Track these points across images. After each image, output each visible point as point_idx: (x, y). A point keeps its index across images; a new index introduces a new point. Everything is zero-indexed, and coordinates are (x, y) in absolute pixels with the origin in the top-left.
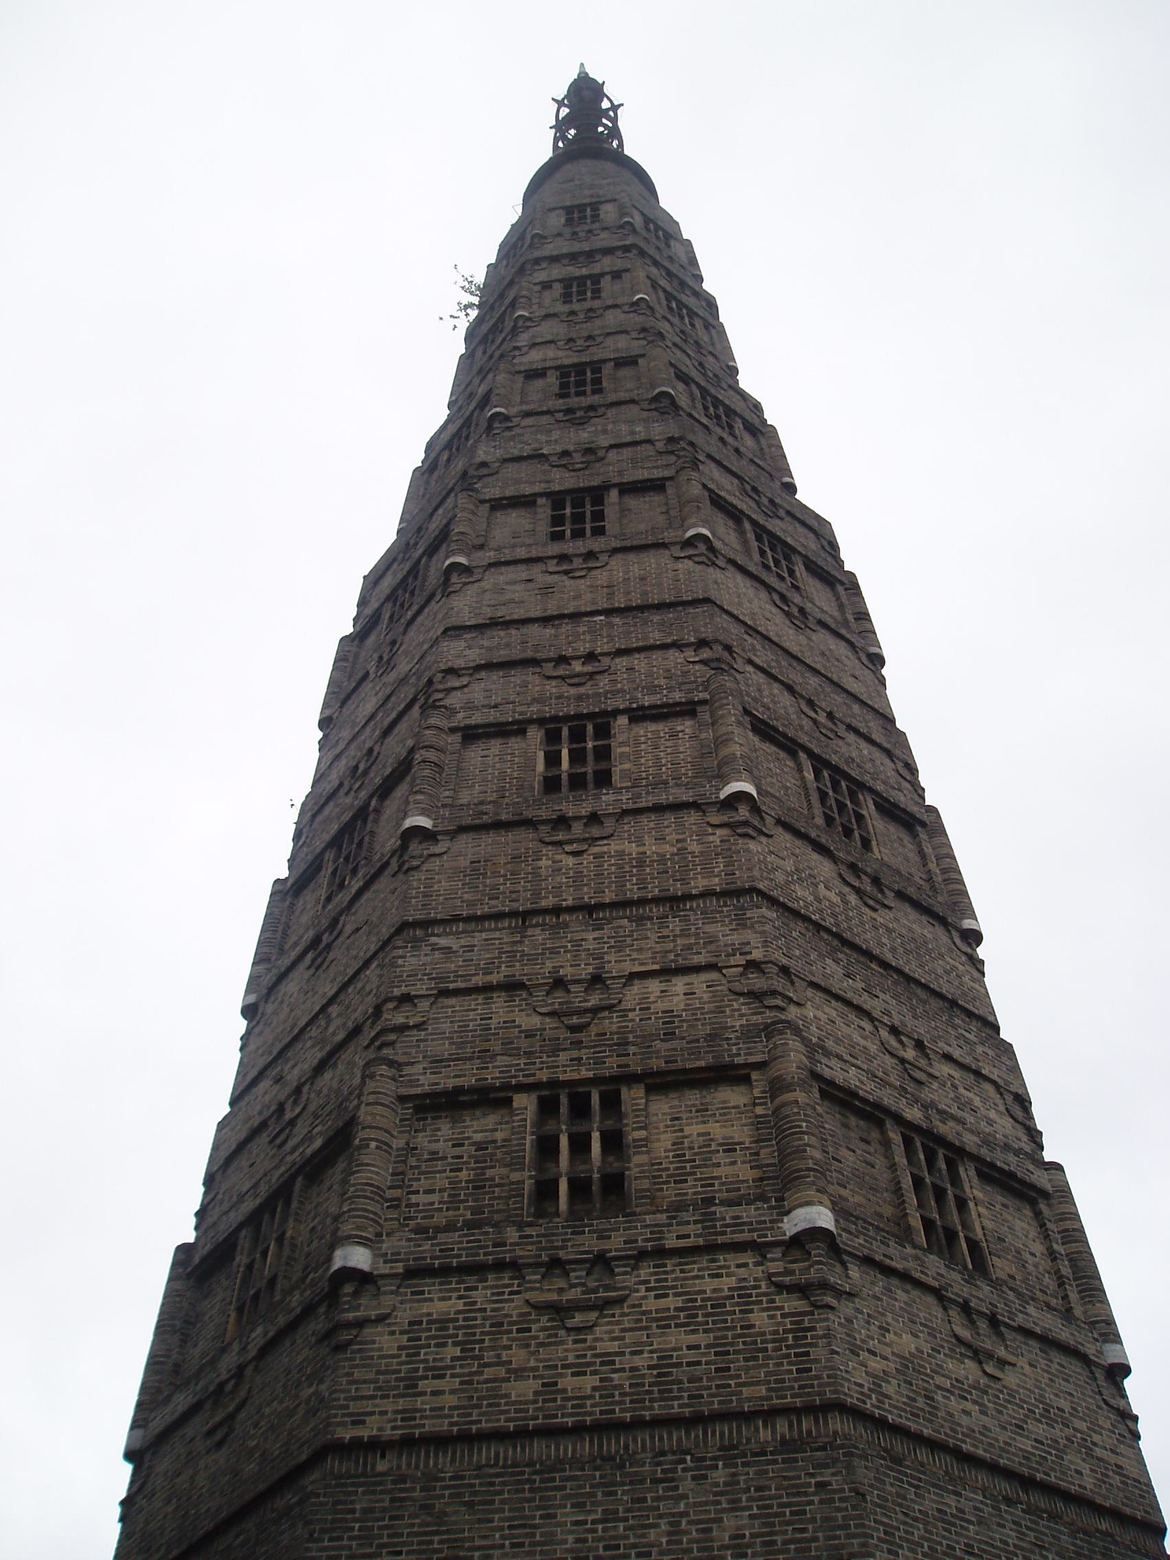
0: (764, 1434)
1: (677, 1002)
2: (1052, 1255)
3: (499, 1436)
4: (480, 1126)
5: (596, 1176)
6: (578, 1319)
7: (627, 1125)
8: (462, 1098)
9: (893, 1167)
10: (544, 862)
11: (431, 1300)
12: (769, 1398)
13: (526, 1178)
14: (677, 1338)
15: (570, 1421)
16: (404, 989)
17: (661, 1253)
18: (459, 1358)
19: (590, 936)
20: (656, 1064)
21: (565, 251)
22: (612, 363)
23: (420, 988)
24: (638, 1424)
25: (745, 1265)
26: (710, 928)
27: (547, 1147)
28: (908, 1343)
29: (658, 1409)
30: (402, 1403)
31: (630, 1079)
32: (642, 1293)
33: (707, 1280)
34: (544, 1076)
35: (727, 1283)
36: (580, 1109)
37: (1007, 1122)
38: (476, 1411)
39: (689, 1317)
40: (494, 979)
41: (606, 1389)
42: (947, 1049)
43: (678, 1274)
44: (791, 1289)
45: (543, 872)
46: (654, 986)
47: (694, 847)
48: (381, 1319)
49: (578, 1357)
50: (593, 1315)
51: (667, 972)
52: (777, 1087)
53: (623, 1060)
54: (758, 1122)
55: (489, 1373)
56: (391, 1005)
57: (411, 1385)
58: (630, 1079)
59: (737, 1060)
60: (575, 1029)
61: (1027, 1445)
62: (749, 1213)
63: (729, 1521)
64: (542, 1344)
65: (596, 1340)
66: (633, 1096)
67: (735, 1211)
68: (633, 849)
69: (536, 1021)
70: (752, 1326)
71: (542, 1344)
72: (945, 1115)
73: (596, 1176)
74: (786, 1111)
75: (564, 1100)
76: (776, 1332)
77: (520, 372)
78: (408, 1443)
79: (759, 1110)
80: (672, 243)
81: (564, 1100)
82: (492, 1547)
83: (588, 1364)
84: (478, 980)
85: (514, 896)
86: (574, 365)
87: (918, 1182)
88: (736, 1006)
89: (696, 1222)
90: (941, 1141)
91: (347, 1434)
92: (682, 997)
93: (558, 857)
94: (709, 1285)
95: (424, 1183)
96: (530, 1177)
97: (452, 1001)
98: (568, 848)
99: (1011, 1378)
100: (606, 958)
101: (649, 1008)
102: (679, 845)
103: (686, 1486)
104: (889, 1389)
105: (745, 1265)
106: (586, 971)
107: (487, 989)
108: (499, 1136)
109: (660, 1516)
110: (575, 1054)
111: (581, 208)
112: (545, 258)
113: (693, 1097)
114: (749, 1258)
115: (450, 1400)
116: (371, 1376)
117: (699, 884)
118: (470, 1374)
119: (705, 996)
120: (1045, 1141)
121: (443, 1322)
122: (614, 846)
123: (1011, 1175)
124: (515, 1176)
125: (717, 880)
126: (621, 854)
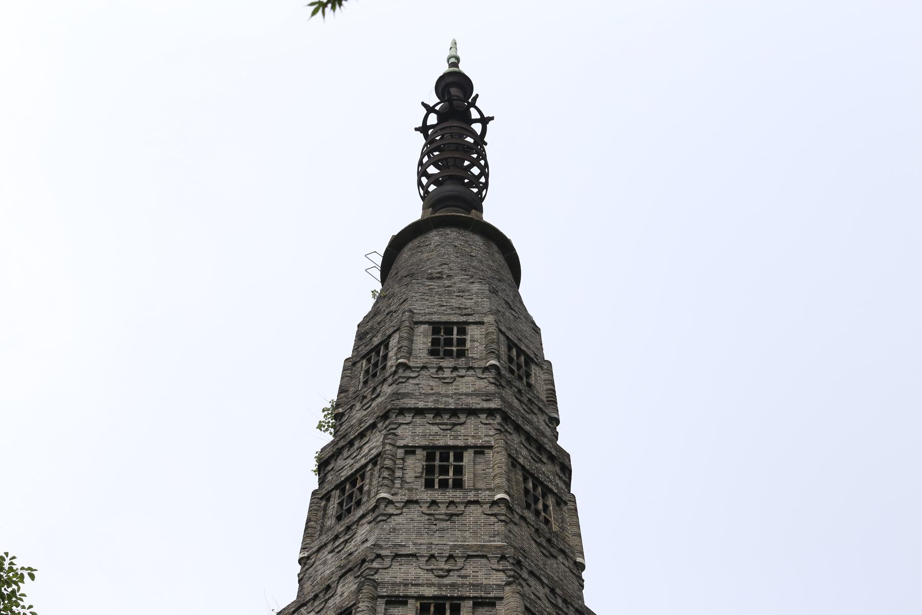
21: (431, 405)
22: (471, 602)
77: (383, 597)
80: (534, 370)
86: (434, 598)
111: (448, 327)
112: (409, 410)
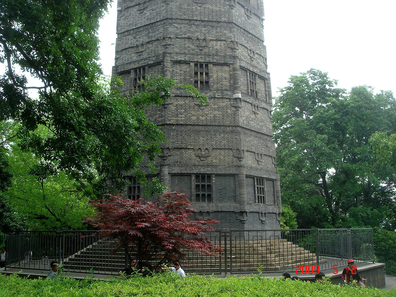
0: (228, 129)
1: (218, 47)
2: (266, 90)
3: (191, 125)
4: (185, 67)
5: (204, 81)
6: (202, 108)
7: (209, 72)
8: (181, 62)
9: (247, 80)
10: (194, 7)
11: (179, 101)
12: (229, 124)
13: (193, 80)
14: (217, 112)
15: (201, 124)
16: (170, 36)
17: (215, 98)
18: (184, 112)
19: (203, 29)
20: (215, 61)
23: (172, 36)
24: (211, 125)
25: (227, 101)
26: (225, 31)
27: (196, 73)
28: (247, 113)
29: (214, 124)
30: (176, 118)
31: (211, 63)
32: (212, 104)
33: (221, 103)
34: (196, 60)
35: (224, 104)
36: (201, 66)
37: (263, 65)
38: (187, 121)
39: (218, 109)
40: (186, 36)
41: (206, 119)
42: (257, 51)
43: (217, 101)
44: (234, 107)
45: (194, 10)
46: (214, 43)
47: (222, 10)
48: (171, 104)
49: (202, 114)
50: (205, 107)
51: (217, 40)
52: (234, 69)
53: (209, 59)
54: (230, 75)
55: (189, 115)
56: (167, 39)
57: (177, 115)
58: (211, 63)
59: (229, 62)
60: (201, 50)
61: (259, 127)
62: (229, 93)
63: (223, 142)
64: (197, 111)
65: (205, 111)
66: (210, 66)
67: (227, 92)
68: (211, 7)
69: (193, 47)
70: (228, 112)
71: (197, 111)
72: (256, 67)
73: (204, 81)
74: (236, 75)
75: (199, 65)
76: (231, 113)
78: (177, 125)
79: (231, 73)
81: (199, 65)
82: (191, 142)
83: (204, 115)
84: (183, 36)
85: (188, 15)
87: (250, 81)
88: (228, 50)
89: (220, 93)
90: (254, 73)
91: (168, 123)
92: (219, 46)
93: (197, 7)
94: (222, 104)
95: (175, 78)
96: (194, 80)
97: (178, 39)
98: (199, 5)
99: (258, 116)
100: (206, 35)
101: (213, 48)
102: (220, 8)
103: (218, 136)
104: (245, 122)
105: (227, 101)
106: (203, 38)
107: (185, 38)
108: (188, 70)
109: (214, 140)
110: (201, 56)
113: (220, 67)
114: (228, 100)
115: (183, 119)
116: (171, 113)
117: (223, 19)
118: (186, 115)
119: (223, 47)
120: (268, 67)
121: (181, 105)
122: (207, 6)
123: (263, 77)
124: (191, 80)
125: (226, 19)
126: (209, 8)
